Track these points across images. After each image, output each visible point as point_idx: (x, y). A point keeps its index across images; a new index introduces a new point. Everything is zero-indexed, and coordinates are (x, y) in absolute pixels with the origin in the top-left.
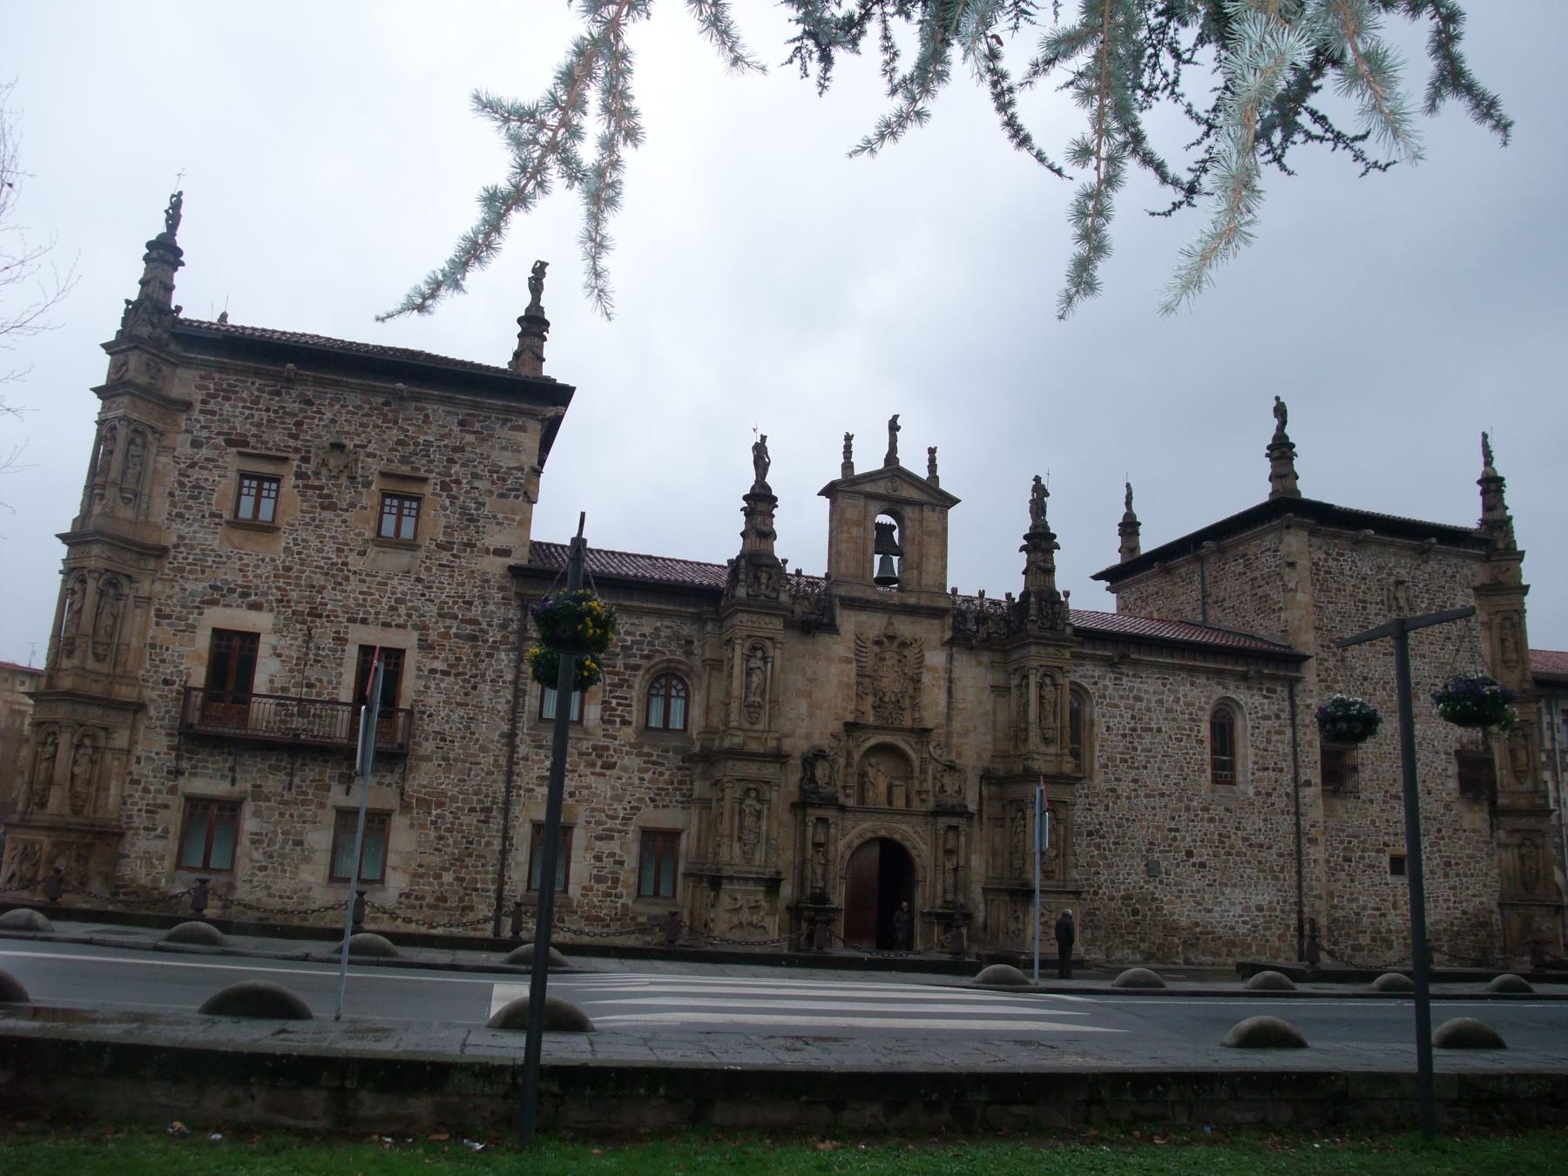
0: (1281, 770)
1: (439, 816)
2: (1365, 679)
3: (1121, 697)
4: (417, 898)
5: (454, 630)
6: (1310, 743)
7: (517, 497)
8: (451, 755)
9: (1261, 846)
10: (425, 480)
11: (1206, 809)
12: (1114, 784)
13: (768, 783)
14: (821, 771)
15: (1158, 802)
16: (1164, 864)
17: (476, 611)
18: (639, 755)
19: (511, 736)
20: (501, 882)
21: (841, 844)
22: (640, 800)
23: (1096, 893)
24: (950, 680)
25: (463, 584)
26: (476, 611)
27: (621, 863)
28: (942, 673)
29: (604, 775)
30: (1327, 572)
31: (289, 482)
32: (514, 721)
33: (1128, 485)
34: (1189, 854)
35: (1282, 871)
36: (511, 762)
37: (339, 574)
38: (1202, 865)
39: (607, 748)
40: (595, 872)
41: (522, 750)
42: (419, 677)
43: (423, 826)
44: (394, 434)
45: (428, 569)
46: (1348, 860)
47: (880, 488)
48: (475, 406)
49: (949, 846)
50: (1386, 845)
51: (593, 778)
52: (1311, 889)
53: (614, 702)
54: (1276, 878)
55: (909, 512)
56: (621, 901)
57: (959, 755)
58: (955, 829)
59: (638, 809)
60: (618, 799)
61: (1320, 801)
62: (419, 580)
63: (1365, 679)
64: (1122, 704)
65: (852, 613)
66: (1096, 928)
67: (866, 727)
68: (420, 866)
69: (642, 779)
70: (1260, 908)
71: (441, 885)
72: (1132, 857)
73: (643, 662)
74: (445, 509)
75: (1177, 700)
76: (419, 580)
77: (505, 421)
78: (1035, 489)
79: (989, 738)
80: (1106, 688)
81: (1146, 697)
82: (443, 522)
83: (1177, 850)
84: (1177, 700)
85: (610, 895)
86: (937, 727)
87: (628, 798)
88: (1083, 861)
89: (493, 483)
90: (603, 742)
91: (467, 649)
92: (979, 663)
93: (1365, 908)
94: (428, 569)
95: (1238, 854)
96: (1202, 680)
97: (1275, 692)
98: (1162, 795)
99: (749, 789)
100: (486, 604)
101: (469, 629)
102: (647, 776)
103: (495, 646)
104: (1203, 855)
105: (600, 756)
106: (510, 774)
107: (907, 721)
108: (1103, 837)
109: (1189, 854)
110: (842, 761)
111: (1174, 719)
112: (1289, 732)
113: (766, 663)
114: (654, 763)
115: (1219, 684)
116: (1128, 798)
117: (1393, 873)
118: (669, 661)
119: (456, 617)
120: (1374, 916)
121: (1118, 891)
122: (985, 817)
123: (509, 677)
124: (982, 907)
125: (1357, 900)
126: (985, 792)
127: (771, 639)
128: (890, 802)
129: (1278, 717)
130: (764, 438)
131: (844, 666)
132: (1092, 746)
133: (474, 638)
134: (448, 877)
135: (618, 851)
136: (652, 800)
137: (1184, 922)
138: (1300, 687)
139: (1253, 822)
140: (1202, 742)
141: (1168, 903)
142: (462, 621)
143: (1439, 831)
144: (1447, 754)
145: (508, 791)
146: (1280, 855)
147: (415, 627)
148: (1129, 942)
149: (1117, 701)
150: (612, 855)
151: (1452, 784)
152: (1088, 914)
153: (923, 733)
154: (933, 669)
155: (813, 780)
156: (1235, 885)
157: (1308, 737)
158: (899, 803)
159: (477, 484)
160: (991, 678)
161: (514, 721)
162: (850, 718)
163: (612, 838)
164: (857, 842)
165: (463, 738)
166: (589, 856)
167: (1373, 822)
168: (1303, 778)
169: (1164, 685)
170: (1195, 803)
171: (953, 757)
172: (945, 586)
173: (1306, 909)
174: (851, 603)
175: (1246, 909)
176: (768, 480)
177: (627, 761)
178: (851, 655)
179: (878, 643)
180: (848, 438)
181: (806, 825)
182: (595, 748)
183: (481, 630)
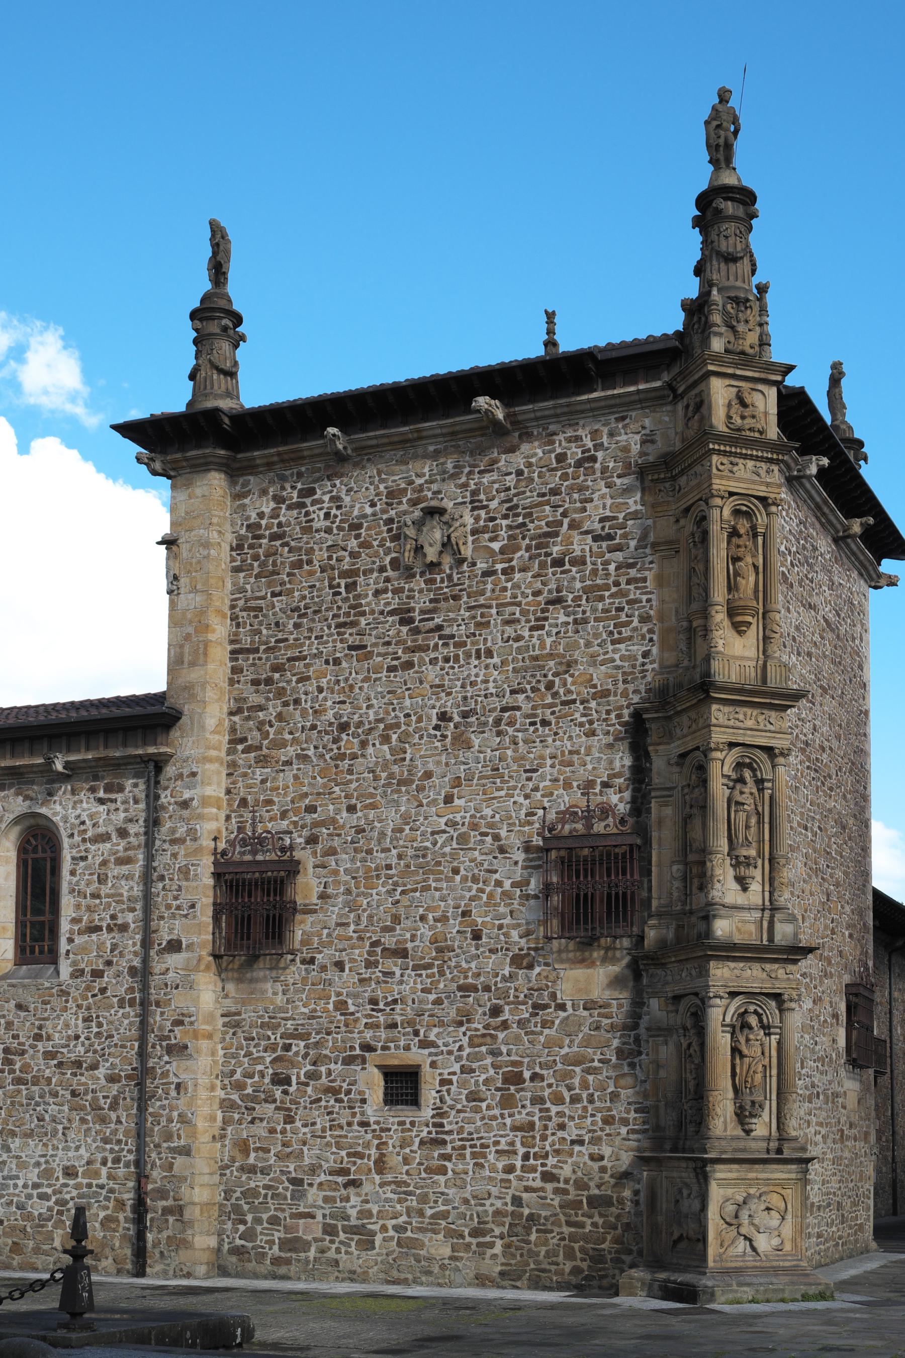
0: (124, 928)
2: (344, 727)
6: (185, 872)
9: (78, 1064)
30: (274, 537)
35: (114, 1106)
46: (281, 1080)
50: (368, 1048)
52: (168, 1137)
54: (103, 1120)
63: (344, 727)
70: (70, 1172)
93: (313, 1170)
97: (121, 789)
120: (334, 1186)
129: (123, 833)
138: (170, 770)
139: (65, 1024)
143: (496, 1011)
146: (112, 1079)
156: (29, 1135)
167: (341, 1006)
173: (156, 1174)
175: (47, 1173)
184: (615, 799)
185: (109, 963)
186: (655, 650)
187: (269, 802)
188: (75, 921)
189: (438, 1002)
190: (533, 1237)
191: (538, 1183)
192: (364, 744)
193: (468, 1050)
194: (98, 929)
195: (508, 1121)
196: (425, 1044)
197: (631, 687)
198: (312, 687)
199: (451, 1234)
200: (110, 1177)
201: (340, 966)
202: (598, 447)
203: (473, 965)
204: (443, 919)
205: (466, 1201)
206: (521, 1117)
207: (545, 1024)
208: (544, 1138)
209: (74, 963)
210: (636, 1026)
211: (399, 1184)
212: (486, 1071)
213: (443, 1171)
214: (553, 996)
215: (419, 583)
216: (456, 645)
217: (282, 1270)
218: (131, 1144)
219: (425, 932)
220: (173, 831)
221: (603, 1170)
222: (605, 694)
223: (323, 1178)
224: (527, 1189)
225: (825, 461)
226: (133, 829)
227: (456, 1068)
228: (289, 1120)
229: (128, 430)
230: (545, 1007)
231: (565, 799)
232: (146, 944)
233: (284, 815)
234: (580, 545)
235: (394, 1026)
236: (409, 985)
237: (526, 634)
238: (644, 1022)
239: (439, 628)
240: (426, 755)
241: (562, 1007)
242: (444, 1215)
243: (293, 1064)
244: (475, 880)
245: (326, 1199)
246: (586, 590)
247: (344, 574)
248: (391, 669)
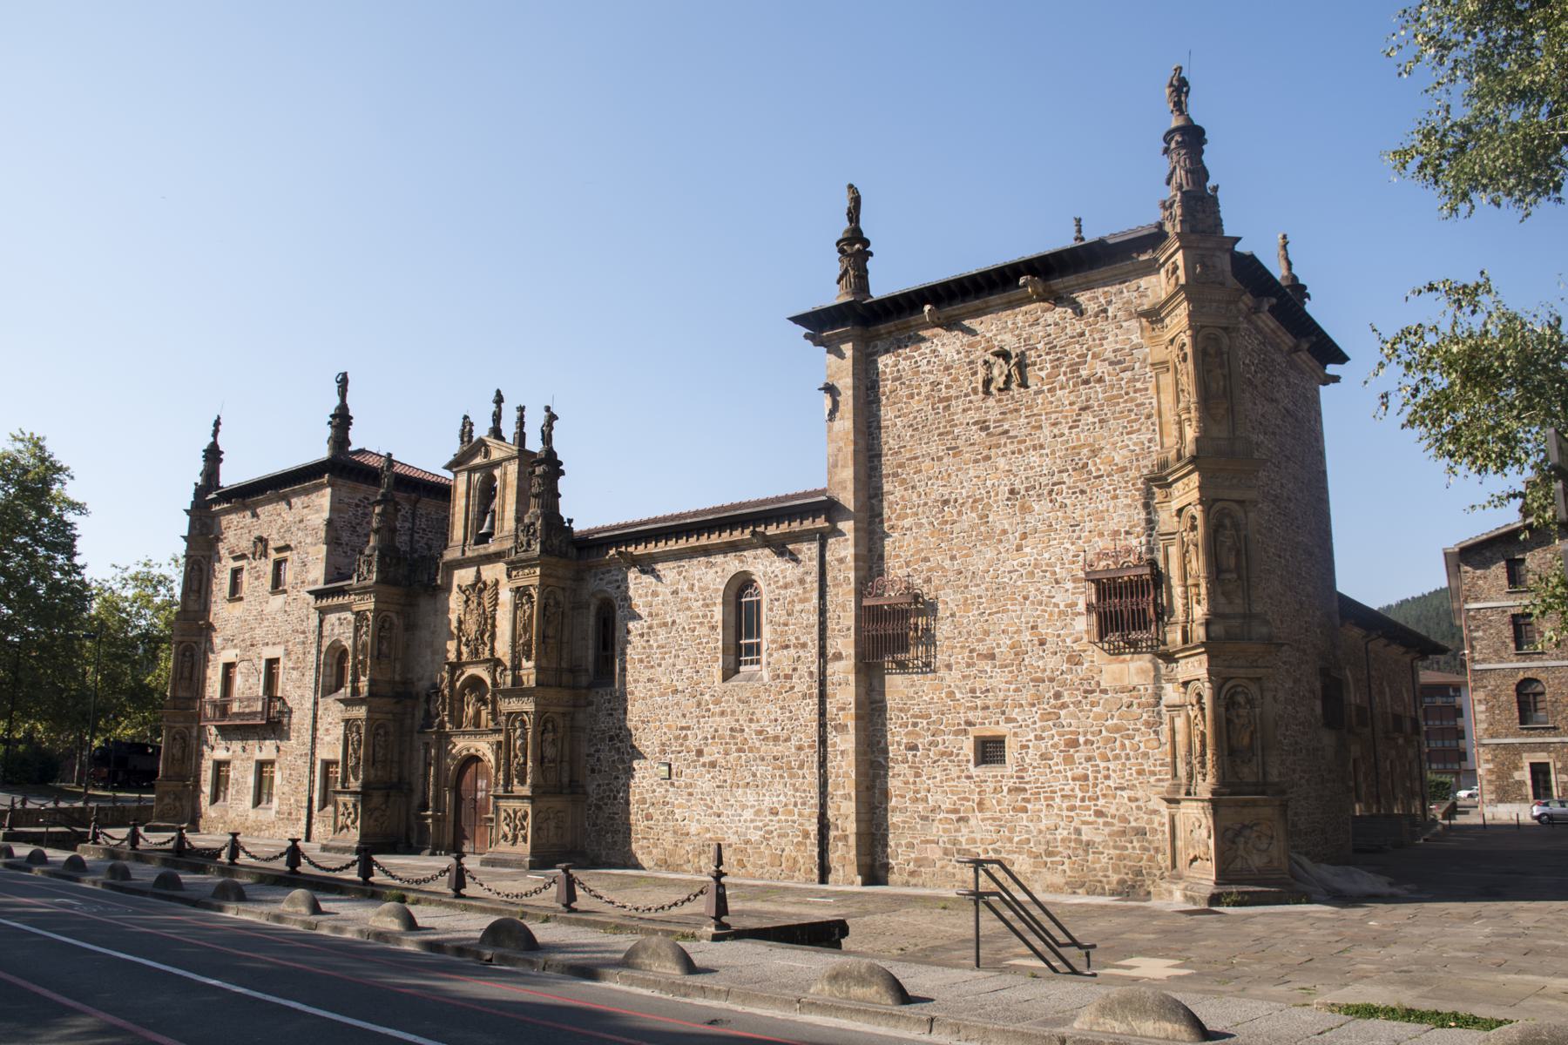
0: (804, 645)
2: (946, 502)
9: (776, 739)
11: (717, 702)
19: (316, 703)
20: (311, 800)
23: (615, 798)
30: (894, 380)
31: (246, 567)
32: (316, 692)
35: (801, 767)
37: (261, 616)
38: (713, 765)
44: (280, 521)
46: (914, 748)
50: (969, 723)
54: (792, 776)
61: (852, 678)
63: (946, 502)
75: (691, 588)
84: (691, 588)
95: (751, 750)
98: (676, 691)
104: (713, 752)
106: (315, 729)
109: (700, 753)
111: (689, 608)
112: (815, 600)
117: (977, 764)
125: (925, 800)
129: (802, 582)
140: (713, 628)
141: (680, 805)
143: (1058, 696)
144: (1075, 580)
146: (800, 748)
151: (1083, 624)
157: (840, 600)
167: (951, 694)
168: (830, 651)
169: (680, 573)
170: (707, 697)
175: (758, 812)
184: (1134, 542)
185: (795, 670)
186: (1158, 437)
187: (898, 556)
188: (773, 642)
189: (1017, 690)
190: (1090, 857)
191: (1093, 818)
192: (960, 513)
193: (1039, 724)
194: (787, 647)
195: (1069, 774)
196: (1009, 720)
197: (1142, 463)
198: (923, 476)
199: (1030, 852)
200: (800, 815)
201: (949, 667)
202: (1109, 303)
203: (1040, 663)
204: (1018, 632)
205: (1040, 832)
206: (1079, 771)
207: (1093, 704)
208: (1095, 785)
209: (774, 670)
210: (1158, 704)
211: (994, 819)
212: (1054, 738)
213: (1025, 810)
214: (1098, 684)
215: (991, 402)
216: (1020, 442)
217: (913, 881)
218: (815, 792)
219: (1006, 641)
220: (835, 578)
221: (1139, 808)
222: (1124, 469)
223: (942, 815)
224: (1084, 823)
225: (1274, 301)
226: (808, 579)
227: (1032, 736)
228: (917, 775)
229: (798, 320)
230: (1092, 692)
231: (1101, 544)
232: (822, 653)
233: (908, 564)
234: (1101, 368)
235: (987, 708)
236: (999, 679)
237: (1066, 432)
238: (1163, 702)
239: (1007, 432)
240: (1001, 518)
241: (1104, 691)
242: (1028, 841)
243: (918, 735)
244: (1040, 604)
245: (945, 830)
246: (1109, 399)
247: (940, 401)
248: (976, 461)
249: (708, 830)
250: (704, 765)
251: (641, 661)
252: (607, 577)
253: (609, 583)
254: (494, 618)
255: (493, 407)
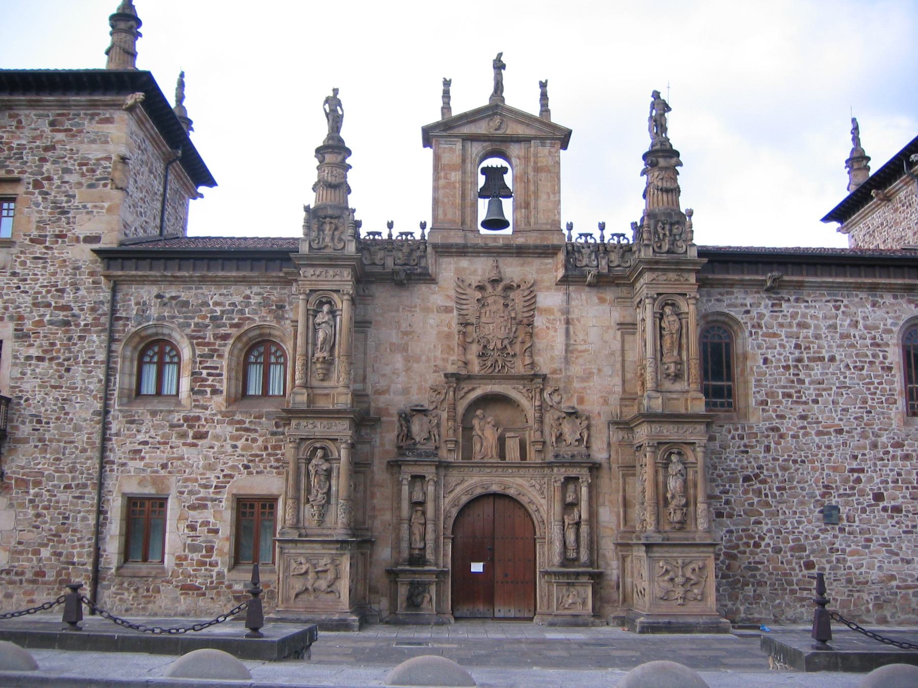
1: (36, 495)
3: (781, 325)
4: (17, 574)
5: (48, 318)
7: (105, 185)
8: (47, 436)
10: (17, 181)
11: (899, 445)
12: (776, 422)
13: (334, 440)
14: (418, 427)
15: (834, 439)
16: (844, 510)
17: (68, 298)
18: (231, 423)
20: (97, 554)
21: (445, 503)
22: (234, 467)
23: (757, 545)
24: (568, 322)
25: (54, 274)
26: (68, 298)
27: (216, 531)
28: (558, 315)
29: (195, 445)
32: (106, 399)
33: (854, 120)
34: (878, 497)
36: (105, 439)
38: (897, 509)
39: (198, 418)
40: (189, 541)
41: (114, 427)
42: (15, 365)
43: (22, 505)
45: (23, 263)
47: (481, 128)
48: (64, 105)
49: (569, 499)
51: (185, 448)
53: (205, 372)
55: (515, 150)
56: (216, 569)
57: (581, 401)
58: (576, 479)
59: (231, 476)
60: (210, 467)
62: (14, 274)
64: (783, 332)
65: (450, 260)
66: (760, 584)
67: (469, 377)
68: (20, 543)
69: (235, 447)
71: (40, 560)
72: (802, 503)
73: (235, 332)
74: (38, 205)
76: (14, 274)
77: (93, 116)
78: (653, 106)
79: (618, 380)
80: (761, 316)
81: (812, 322)
82: (35, 217)
83: (862, 493)
84: (855, 324)
85: (203, 564)
86: (554, 372)
87: (220, 467)
88: (739, 510)
89: (83, 175)
90: (197, 412)
91: (60, 334)
92: (602, 301)
94: (23, 263)
96: (888, 299)
98: (840, 431)
99: (316, 449)
100: (78, 289)
101: (61, 315)
102: (240, 444)
103: (86, 329)
105: (191, 427)
106: (103, 449)
107: (519, 367)
108: (764, 482)
109: (878, 497)
110: (445, 415)
111: (852, 346)
113: (334, 317)
114: (247, 430)
115: (910, 302)
116: (793, 437)
118: (259, 327)
119: (48, 305)
121: (786, 541)
122: (614, 466)
123: (101, 356)
124: (614, 564)
126: (614, 440)
127: (337, 291)
128: (502, 456)
130: (336, 91)
131: (444, 316)
132: (746, 382)
133: (67, 323)
134: (45, 553)
135: (212, 520)
136: (246, 467)
137: (875, 574)
140: (890, 369)
141: (852, 553)
142: (56, 308)
145: (102, 467)
147: (11, 318)
148: (802, 599)
149: (775, 329)
150: (207, 523)
152: (749, 568)
153: (535, 379)
154: (548, 311)
155: (409, 436)
158: (513, 453)
159: (67, 177)
160: (618, 315)
161: (106, 399)
162: (451, 369)
163: (205, 507)
164: (464, 499)
165: (58, 418)
166: (182, 526)
169: (837, 308)
170: (884, 439)
171: (574, 402)
172: (559, 222)
174: (445, 250)
176: (343, 134)
177: (219, 429)
178: (451, 304)
179: (481, 288)
180: (447, 83)
181: (400, 483)
182: (186, 419)
183: (74, 316)
249: (893, 577)
250: (885, 509)
251: (786, 395)
252: (727, 300)
253: (735, 306)
254: (530, 324)
255: (491, 73)
